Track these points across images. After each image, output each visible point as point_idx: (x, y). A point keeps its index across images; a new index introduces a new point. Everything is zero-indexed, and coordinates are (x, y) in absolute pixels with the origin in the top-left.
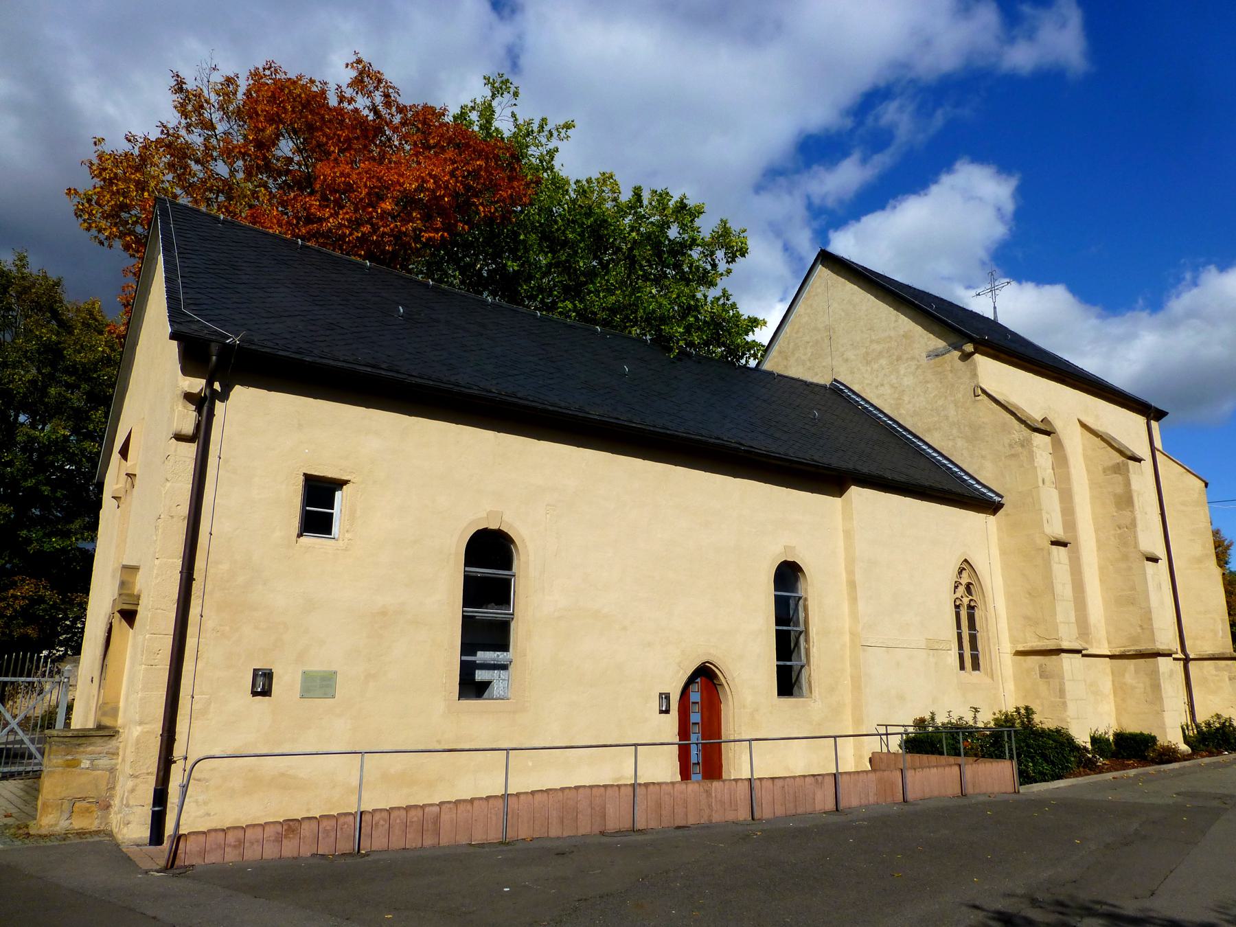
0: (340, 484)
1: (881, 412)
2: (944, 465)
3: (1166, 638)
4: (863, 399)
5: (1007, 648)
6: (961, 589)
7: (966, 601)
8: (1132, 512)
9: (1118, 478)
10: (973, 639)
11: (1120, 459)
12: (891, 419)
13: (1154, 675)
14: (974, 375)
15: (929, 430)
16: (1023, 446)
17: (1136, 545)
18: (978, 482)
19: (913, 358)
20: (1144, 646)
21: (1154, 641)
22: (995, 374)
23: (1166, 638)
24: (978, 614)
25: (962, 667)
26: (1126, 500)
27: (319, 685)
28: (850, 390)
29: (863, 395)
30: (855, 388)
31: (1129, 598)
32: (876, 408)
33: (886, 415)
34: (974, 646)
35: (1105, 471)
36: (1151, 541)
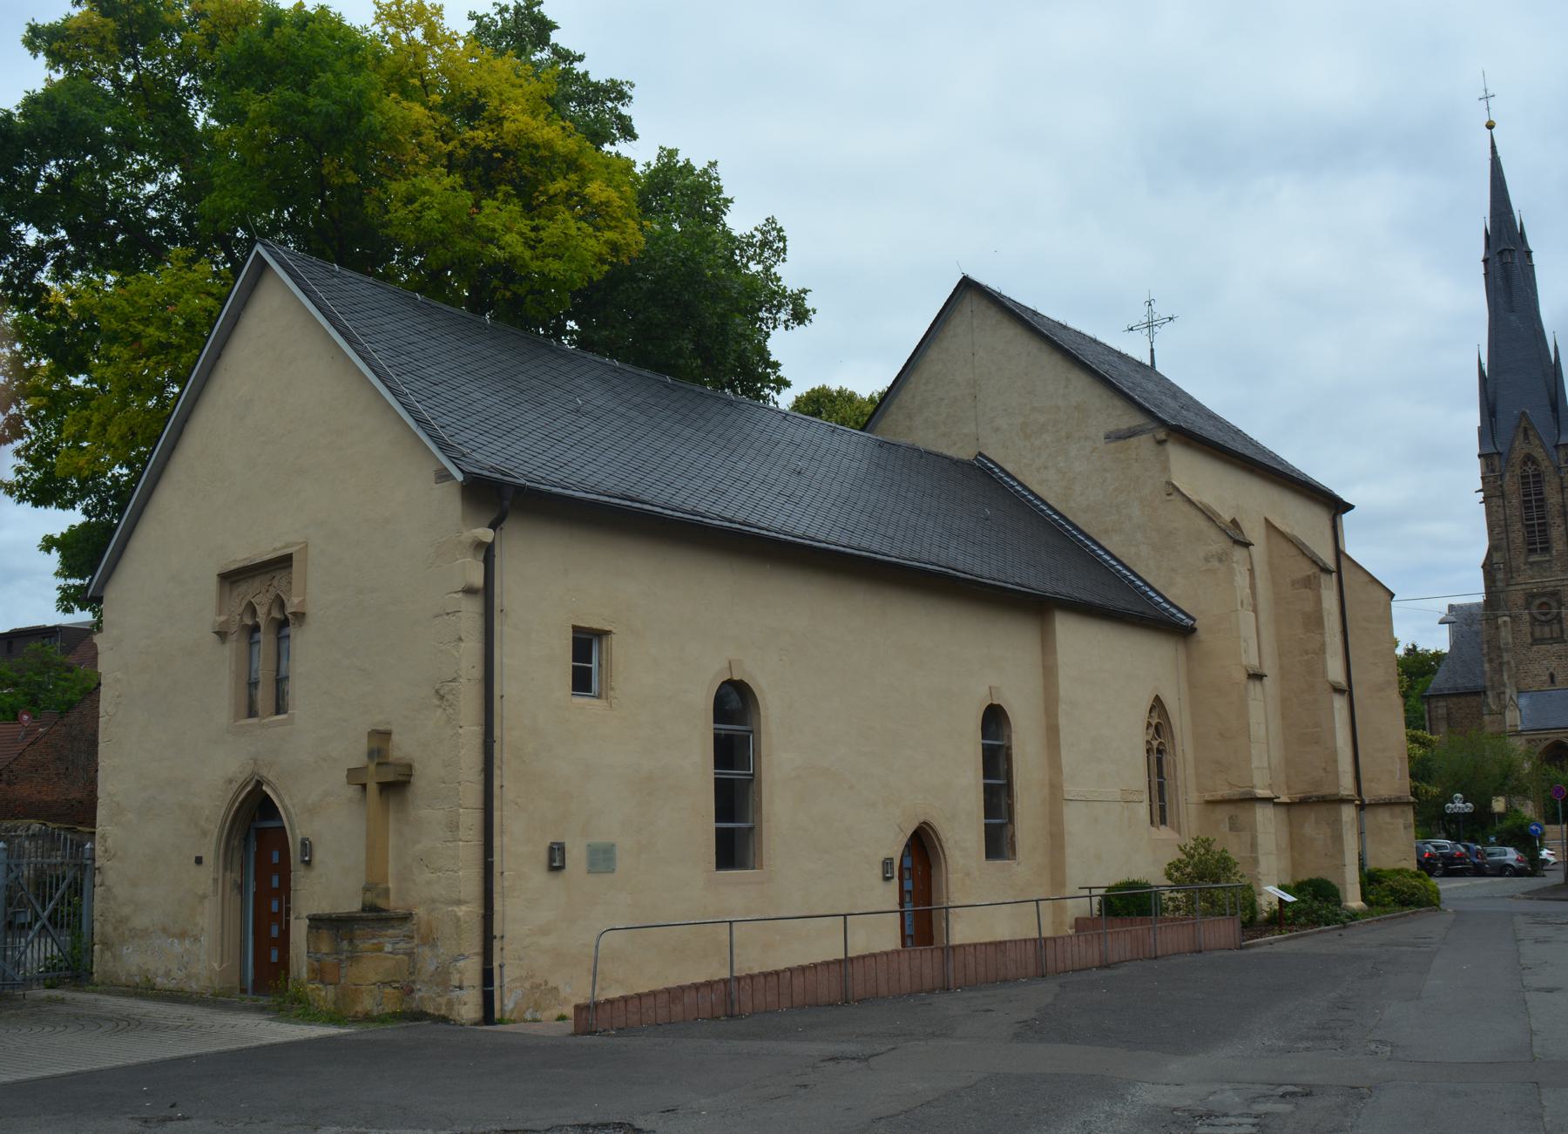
0: (601, 634)
1: (1045, 503)
2: (1125, 577)
3: (1347, 786)
4: (1020, 484)
5: (1194, 797)
6: (1152, 730)
7: (1155, 744)
8: (1322, 635)
9: (1308, 593)
10: (1161, 785)
11: (1313, 570)
12: (1056, 512)
13: (1336, 824)
14: (1166, 469)
15: (1106, 532)
16: (1220, 560)
17: (1325, 672)
18: (1166, 600)
19: (1087, 438)
20: (1326, 790)
21: (1338, 785)
22: (1195, 475)
23: (1347, 786)
24: (1166, 758)
25: (1152, 822)
26: (1315, 621)
27: (602, 859)
28: (1002, 470)
29: (1020, 478)
30: (1009, 468)
31: (1303, 734)
32: (1037, 497)
33: (1050, 507)
34: (1162, 798)
35: (1293, 583)
36: (1335, 672)
